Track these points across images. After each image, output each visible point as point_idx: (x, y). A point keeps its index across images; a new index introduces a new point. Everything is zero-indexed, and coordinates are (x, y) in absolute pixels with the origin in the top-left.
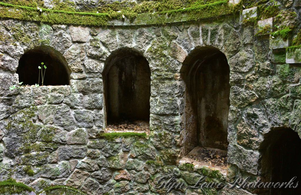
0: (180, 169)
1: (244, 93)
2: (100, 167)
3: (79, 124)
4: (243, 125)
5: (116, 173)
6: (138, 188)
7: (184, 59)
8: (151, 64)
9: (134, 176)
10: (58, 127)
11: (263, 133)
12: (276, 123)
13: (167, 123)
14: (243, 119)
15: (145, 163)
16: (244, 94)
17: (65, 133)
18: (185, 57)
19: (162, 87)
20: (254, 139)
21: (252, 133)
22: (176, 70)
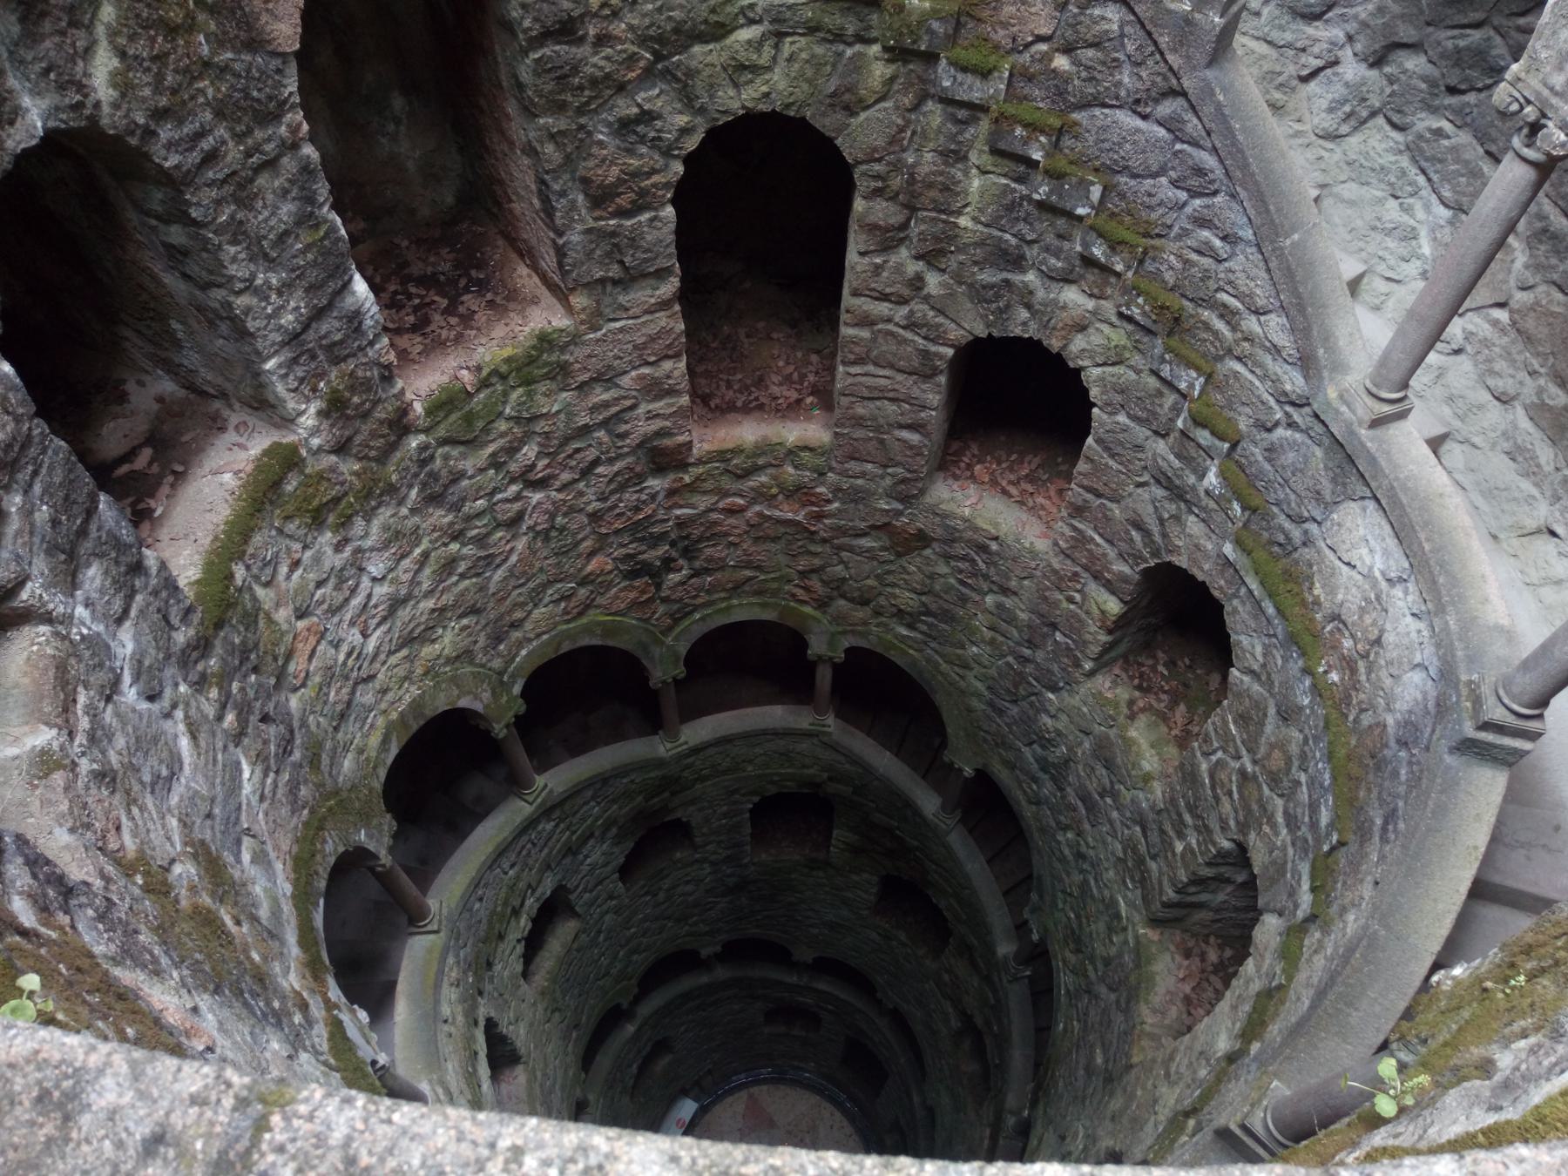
0: (426, 431)
1: (595, 59)
2: (265, 719)
3: (168, 692)
4: (603, 161)
5: (292, 668)
6: (348, 617)
7: (299, 30)
8: (163, 152)
9: (325, 606)
10: (174, 800)
13: (338, 337)
14: (600, 143)
15: (329, 534)
16: (595, 65)
17: (188, 787)
18: (297, 15)
19: (260, 218)
20: (656, 179)
22: (285, 101)
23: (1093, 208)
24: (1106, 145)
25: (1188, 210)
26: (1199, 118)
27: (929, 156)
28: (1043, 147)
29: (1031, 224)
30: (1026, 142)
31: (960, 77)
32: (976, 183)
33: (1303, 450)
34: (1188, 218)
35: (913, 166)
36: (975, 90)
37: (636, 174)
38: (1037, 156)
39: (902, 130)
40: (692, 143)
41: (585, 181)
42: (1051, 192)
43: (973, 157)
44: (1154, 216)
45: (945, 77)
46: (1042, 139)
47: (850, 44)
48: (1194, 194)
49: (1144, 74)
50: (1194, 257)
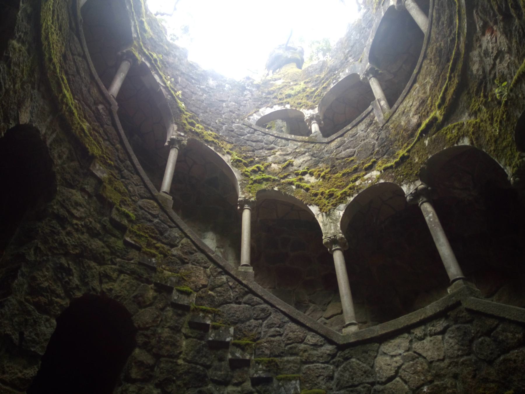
11: (73, 296)
12: (94, 290)
20: (58, 300)
21: (57, 292)
23: (232, 337)
24: (231, 315)
25: (264, 325)
26: (257, 295)
27: (167, 330)
28: (210, 319)
29: (207, 357)
30: (204, 317)
31: (180, 296)
32: (184, 343)
33: (348, 366)
34: (265, 327)
35: (160, 334)
36: (185, 301)
37: (53, 292)
38: (208, 322)
39: (158, 317)
40: (79, 294)
41: (34, 279)
42: (216, 335)
43: (183, 331)
44: (254, 332)
45: (175, 296)
46: (210, 315)
47: (143, 283)
48: (263, 319)
49: (237, 290)
50: (272, 339)
